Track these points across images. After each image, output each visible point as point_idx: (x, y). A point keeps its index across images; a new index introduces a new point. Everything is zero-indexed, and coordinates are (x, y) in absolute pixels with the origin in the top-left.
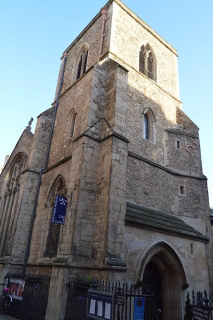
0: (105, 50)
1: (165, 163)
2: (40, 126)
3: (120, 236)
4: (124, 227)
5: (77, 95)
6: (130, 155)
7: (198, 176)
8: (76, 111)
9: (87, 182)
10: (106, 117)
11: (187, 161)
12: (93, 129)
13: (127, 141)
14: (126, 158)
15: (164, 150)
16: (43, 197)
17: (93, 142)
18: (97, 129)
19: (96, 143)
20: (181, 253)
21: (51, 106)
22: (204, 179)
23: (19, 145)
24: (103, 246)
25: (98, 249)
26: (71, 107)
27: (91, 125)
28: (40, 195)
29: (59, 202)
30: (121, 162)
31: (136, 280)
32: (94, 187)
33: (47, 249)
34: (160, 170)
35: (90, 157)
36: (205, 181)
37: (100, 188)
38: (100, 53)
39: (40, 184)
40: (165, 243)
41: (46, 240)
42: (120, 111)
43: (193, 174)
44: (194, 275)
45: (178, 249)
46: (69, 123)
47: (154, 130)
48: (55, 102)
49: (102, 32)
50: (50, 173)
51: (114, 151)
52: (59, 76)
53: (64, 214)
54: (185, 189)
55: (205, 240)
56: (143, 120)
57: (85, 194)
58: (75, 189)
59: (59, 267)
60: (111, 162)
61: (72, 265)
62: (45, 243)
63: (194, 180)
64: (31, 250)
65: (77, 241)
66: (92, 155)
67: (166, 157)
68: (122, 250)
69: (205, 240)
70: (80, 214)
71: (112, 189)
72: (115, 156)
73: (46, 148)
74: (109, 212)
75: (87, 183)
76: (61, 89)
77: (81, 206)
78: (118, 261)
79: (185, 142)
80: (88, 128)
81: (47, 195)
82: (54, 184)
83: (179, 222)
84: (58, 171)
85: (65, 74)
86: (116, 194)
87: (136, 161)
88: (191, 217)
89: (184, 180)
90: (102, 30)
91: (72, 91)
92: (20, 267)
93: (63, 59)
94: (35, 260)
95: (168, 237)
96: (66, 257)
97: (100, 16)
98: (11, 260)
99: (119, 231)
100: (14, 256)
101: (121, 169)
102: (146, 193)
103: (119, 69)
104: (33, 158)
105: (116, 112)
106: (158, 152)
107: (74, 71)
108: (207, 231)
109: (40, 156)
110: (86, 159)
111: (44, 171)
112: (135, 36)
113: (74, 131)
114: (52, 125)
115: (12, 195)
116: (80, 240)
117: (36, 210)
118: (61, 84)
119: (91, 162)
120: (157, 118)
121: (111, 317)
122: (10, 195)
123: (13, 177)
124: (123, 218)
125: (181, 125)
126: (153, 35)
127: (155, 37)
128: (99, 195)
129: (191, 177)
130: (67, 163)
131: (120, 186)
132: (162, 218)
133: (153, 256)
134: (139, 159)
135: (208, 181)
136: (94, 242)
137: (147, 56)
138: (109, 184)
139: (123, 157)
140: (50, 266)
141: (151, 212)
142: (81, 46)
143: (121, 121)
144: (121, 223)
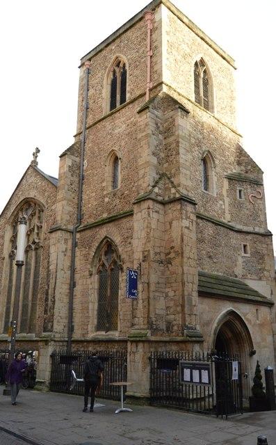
1: (226, 219)
2: (66, 169)
6: (199, 217)
7: (262, 231)
8: (119, 155)
12: (156, 190)
13: (195, 204)
14: (194, 223)
18: (160, 189)
19: (160, 206)
20: (247, 320)
22: (269, 235)
23: (22, 188)
24: (180, 320)
25: (175, 322)
27: (153, 184)
28: (77, 259)
29: (130, 276)
32: (163, 257)
33: (98, 322)
34: (222, 228)
35: (156, 224)
36: (270, 237)
39: (75, 245)
41: (96, 313)
43: (257, 230)
45: (245, 315)
46: (108, 169)
50: (88, 233)
52: (80, 94)
53: (136, 288)
54: (248, 248)
55: (270, 305)
56: (201, 168)
57: (155, 265)
58: (143, 261)
59: (137, 342)
60: (182, 231)
61: (153, 338)
62: (96, 316)
63: (258, 236)
65: (152, 315)
67: (227, 211)
69: (270, 305)
70: (152, 288)
71: (185, 260)
72: (186, 223)
74: (183, 284)
75: (156, 254)
77: (154, 278)
79: (248, 190)
80: (150, 188)
82: (98, 247)
84: (102, 232)
89: (247, 237)
92: (65, 344)
93: (85, 68)
95: (236, 305)
96: (143, 332)
97: (141, 19)
99: (194, 303)
100: (57, 332)
101: (191, 236)
102: (210, 257)
104: (61, 210)
108: (272, 294)
109: (71, 209)
110: (153, 227)
112: (188, 51)
114: (80, 167)
116: (156, 314)
118: (85, 108)
120: (217, 162)
121: (209, 380)
125: (242, 167)
126: (208, 44)
127: (210, 46)
128: (170, 266)
130: (116, 223)
131: (192, 256)
132: (229, 284)
136: (167, 315)
138: (181, 254)
141: (217, 278)
142: (114, 57)
144: (195, 294)
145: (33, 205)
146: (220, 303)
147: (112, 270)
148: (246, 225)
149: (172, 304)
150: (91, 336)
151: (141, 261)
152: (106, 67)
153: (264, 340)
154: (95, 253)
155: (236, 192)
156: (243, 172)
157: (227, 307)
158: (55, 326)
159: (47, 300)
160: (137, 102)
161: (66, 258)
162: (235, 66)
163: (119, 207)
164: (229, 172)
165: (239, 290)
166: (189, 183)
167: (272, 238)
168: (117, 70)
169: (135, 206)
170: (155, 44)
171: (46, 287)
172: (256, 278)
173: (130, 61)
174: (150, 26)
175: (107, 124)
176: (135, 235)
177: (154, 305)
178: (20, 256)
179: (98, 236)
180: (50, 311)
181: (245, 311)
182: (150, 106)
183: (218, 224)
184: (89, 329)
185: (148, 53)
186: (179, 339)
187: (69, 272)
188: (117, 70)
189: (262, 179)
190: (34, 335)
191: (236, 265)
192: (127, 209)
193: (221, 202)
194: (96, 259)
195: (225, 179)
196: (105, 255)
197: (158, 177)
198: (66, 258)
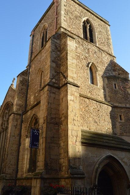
0: (58, 26)
9: (52, 118)
10: (62, 72)
12: (54, 80)
14: (78, 98)
15: (106, 90)
16: (24, 131)
17: (55, 89)
18: (56, 80)
20: (124, 162)
21: (26, 68)
23: (7, 97)
24: (67, 162)
25: (64, 164)
26: (39, 68)
27: (52, 77)
28: (22, 129)
29: (33, 133)
31: (93, 184)
33: (29, 166)
37: (62, 121)
38: (55, 28)
39: (22, 122)
40: (111, 156)
41: (28, 161)
42: (71, 66)
48: (28, 65)
49: (55, 14)
54: (123, 117)
58: (44, 123)
62: (28, 163)
64: (19, 168)
66: (54, 98)
68: (81, 163)
73: (25, 96)
75: (52, 118)
76: (31, 57)
78: (78, 171)
81: (27, 129)
82: (31, 121)
85: (33, 45)
87: (86, 100)
89: (122, 110)
90: (55, 13)
91: (39, 57)
93: (32, 36)
94: (22, 175)
97: (53, 4)
100: (8, 174)
103: (68, 38)
107: (39, 43)
109: (21, 103)
111: (24, 113)
115: (5, 132)
116: (51, 159)
117: (20, 141)
118: (32, 53)
122: (3, 131)
123: (4, 119)
124: (80, 141)
125: (116, 73)
129: (127, 108)
133: (104, 166)
134: (88, 98)
137: (88, 28)
140: (31, 179)
142: (43, 26)
148: (120, 103)
150: (24, 176)
154: (29, 124)
156: (117, 75)
157: (109, 153)
161: (17, 129)
162: (109, 24)
164: (108, 74)
165: (115, 143)
181: (119, 156)
187: (18, 137)
189: (128, 77)
195: (105, 78)
198: (17, 129)
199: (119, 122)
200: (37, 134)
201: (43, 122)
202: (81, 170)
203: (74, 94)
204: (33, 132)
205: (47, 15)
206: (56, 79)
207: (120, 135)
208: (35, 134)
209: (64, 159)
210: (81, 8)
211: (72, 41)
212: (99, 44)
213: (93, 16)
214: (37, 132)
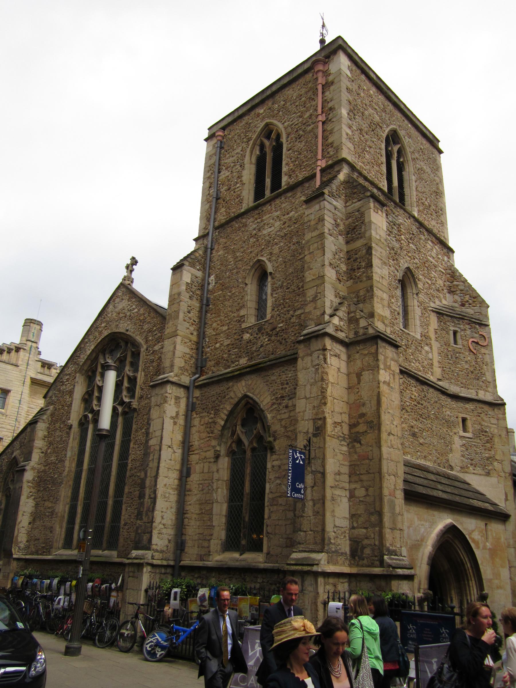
3: (400, 517)
4: (403, 502)
5: (265, 232)
7: (489, 398)
8: (270, 268)
11: (472, 369)
12: (336, 321)
14: (397, 377)
15: (434, 348)
16: (204, 435)
18: (341, 319)
20: (473, 540)
24: (377, 537)
25: (366, 542)
28: (194, 430)
29: (294, 460)
30: (391, 385)
31: (422, 591)
33: (228, 536)
34: (431, 390)
35: (336, 375)
37: (358, 432)
39: (191, 408)
41: (224, 520)
42: (380, 286)
43: (482, 395)
44: (491, 577)
46: (251, 289)
47: (416, 311)
51: (382, 366)
53: (303, 481)
54: (469, 423)
58: (315, 435)
60: (379, 387)
67: (436, 364)
71: (384, 436)
73: (195, 333)
82: (231, 413)
83: (466, 486)
86: (389, 445)
88: (480, 475)
98: (153, 558)
100: (157, 551)
102: (414, 435)
105: (375, 289)
106: (423, 352)
108: (506, 499)
112: (377, 118)
113: (269, 310)
116: (335, 526)
119: (338, 384)
120: (420, 285)
125: (456, 297)
128: (357, 445)
135: (508, 408)
139: (394, 375)
142: (262, 125)
143: (383, 306)
144: (400, 495)
145: (122, 344)
146: (436, 514)
147: (253, 450)
148: (465, 386)
149: (361, 510)
151: (310, 435)
152: (249, 140)
153: (497, 575)
154: (226, 421)
155: (448, 333)
156: (456, 305)
158: (155, 540)
159: (142, 496)
160: (299, 189)
162: (441, 146)
163: (270, 348)
164: (438, 302)
166: (386, 313)
167: (505, 409)
168: (267, 143)
169: (302, 346)
170: (330, 105)
171: (142, 475)
172: (483, 473)
173: (289, 130)
174: (321, 80)
175: (251, 224)
176: (300, 392)
177: (333, 511)
178: (105, 423)
179: (232, 394)
180: (147, 514)
182: (326, 191)
183: (423, 382)
184: (213, 548)
185: (320, 118)
186: (377, 570)
188: (267, 143)
189: (487, 317)
190: (115, 553)
191: (451, 450)
192: (281, 351)
193: (427, 348)
194: (226, 432)
196: (243, 425)
197: (338, 300)
198: (177, 427)
199: (461, 437)
200: (301, 463)
201: (311, 430)
202: (404, 557)
203: (390, 365)
204: (293, 456)
205: (280, 98)
206: (340, 318)
207: (460, 472)
208: (298, 462)
209: (365, 528)
210: (381, 97)
211: (380, 212)
212: (419, 211)
213: (406, 122)
214: (301, 457)
